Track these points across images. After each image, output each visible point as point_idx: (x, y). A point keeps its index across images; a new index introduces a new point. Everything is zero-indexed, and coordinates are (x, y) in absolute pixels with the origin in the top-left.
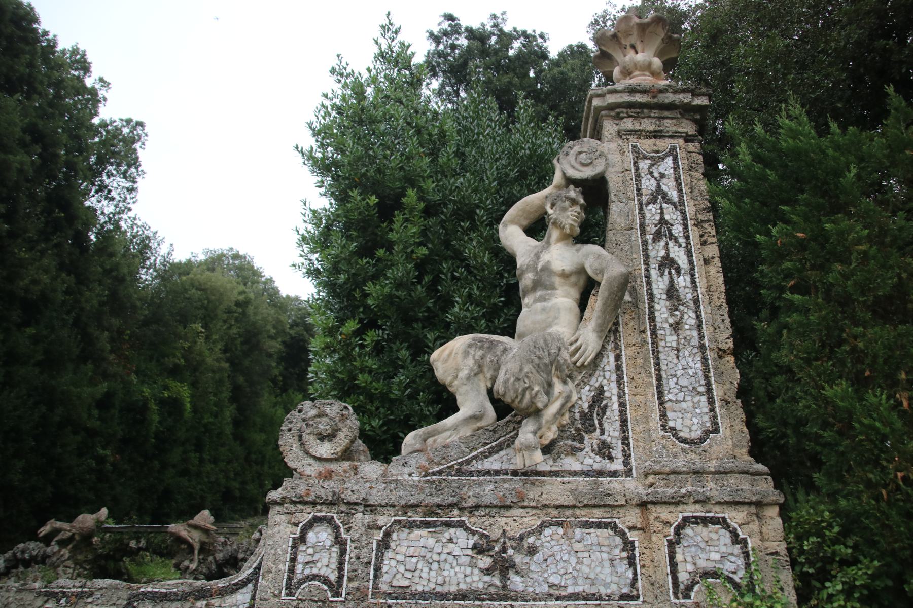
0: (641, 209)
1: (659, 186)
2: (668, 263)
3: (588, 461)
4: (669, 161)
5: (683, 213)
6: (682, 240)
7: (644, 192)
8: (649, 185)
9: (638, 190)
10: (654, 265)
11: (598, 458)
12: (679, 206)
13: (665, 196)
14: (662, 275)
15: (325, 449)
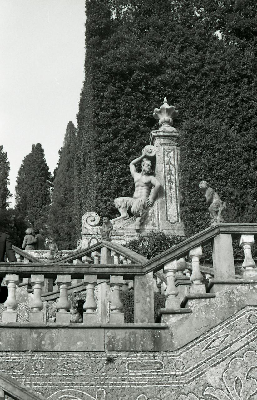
0: (164, 166)
1: (169, 160)
2: (170, 181)
3: (150, 227)
4: (172, 152)
5: (175, 168)
6: (174, 176)
7: (165, 161)
8: (167, 159)
9: (164, 161)
10: (167, 182)
11: (152, 226)
12: (174, 166)
13: (171, 163)
14: (169, 184)
15: (93, 224)
